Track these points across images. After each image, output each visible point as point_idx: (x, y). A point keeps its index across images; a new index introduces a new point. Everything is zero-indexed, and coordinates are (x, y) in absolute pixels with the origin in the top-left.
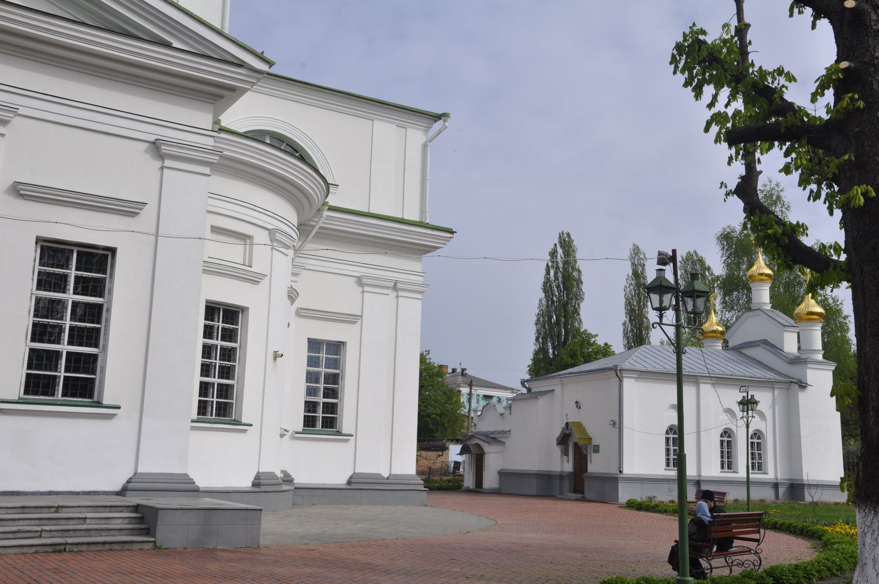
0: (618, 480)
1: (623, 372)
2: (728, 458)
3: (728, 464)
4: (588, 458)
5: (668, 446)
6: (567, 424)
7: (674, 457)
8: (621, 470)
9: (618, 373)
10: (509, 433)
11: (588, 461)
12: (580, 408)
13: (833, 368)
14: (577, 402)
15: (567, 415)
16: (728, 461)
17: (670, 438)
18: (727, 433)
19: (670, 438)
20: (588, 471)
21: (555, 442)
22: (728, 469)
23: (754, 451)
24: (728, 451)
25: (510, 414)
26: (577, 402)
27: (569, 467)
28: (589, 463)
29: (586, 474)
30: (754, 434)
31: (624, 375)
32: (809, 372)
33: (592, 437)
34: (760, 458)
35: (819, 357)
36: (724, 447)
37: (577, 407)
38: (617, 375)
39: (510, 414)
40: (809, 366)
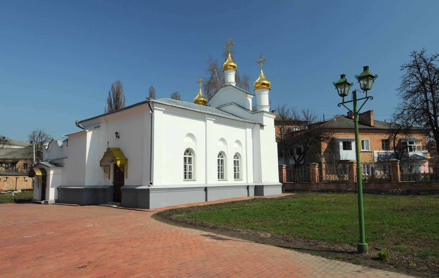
0: (149, 191)
1: (155, 104)
2: (221, 171)
4: (125, 175)
5: (185, 163)
6: (108, 149)
7: (189, 171)
8: (152, 182)
9: (151, 104)
10: (66, 159)
11: (125, 177)
12: (119, 137)
13: (274, 117)
14: (117, 133)
15: (108, 143)
16: (222, 173)
18: (221, 154)
20: (124, 185)
22: (189, 178)
23: (235, 166)
24: (221, 167)
25: (67, 146)
26: (117, 133)
27: (110, 182)
28: (125, 178)
29: (122, 187)
30: (235, 155)
31: (155, 107)
32: (264, 117)
33: (128, 159)
34: (238, 171)
35: (267, 110)
36: (219, 164)
37: (117, 137)
38: (149, 106)
39: (67, 146)
40: (265, 114)
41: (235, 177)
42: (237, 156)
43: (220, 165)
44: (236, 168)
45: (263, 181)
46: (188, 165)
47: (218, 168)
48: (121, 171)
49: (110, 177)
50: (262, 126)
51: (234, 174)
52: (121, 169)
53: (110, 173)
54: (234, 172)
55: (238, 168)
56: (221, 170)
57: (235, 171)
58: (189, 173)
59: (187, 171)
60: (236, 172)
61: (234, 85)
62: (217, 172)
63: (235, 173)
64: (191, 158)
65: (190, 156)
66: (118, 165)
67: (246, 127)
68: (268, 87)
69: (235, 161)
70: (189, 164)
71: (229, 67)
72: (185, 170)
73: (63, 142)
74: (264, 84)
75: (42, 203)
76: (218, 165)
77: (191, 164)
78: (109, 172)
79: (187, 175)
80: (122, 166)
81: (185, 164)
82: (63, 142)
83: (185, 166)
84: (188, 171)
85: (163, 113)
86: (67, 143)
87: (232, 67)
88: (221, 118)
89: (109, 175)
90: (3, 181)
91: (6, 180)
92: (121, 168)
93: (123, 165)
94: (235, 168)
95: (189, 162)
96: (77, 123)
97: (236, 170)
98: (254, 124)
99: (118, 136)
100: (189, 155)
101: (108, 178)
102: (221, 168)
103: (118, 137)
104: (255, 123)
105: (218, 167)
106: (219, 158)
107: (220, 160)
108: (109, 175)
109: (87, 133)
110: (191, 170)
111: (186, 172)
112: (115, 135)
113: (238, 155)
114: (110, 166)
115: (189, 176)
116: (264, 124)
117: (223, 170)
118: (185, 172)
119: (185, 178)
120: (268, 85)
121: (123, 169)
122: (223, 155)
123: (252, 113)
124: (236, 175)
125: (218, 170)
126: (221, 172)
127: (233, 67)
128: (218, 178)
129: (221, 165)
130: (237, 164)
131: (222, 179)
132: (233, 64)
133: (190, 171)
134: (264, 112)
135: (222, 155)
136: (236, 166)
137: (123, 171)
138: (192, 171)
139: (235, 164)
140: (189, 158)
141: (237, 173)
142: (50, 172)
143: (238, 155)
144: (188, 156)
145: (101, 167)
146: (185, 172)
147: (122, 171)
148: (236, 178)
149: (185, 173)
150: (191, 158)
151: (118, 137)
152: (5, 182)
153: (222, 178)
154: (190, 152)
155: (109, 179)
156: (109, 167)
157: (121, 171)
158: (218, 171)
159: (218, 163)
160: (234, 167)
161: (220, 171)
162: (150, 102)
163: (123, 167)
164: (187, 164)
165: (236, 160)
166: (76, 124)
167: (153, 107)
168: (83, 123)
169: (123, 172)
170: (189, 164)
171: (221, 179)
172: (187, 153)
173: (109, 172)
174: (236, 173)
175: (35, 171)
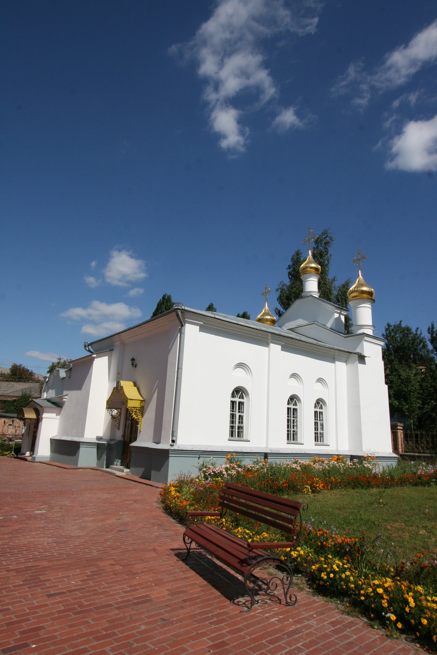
0: (169, 454)
2: (293, 428)
3: (293, 434)
5: (233, 411)
8: (174, 439)
9: (180, 313)
12: (136, 366)
17: (236, 402)
18: (293, 399)
19: (236, 402)
21: (104, 405)
23: (316, 421)
24: (294, 421)
26: (133, 360)
32: (365, 343)
34: (322, 429)
37: (133, 365)
38: (178, 315)
39: (70, 377)
40: (366, 338)
41: (316, 439)
42: (319, 403)
43: (291, 417)
44: (317, 423)
45: (364, 449)
46: (237, 414)
47: (288, 422)
48: (133, 417)
49: (119, 427)
50: (362, 358)
51: (315, 433)
52: (133, 414)
53: (120, 421)
54: (315, 430)
55: (322, 425)
56: (293, 426)
57: (316, 429)
58: (239, 428)
59: (235, 424)
60: (318, 430)
61: (317, 295)
62: (286, 429)
63: (316, 432)
64: (244, 402)
65: (241, 400)
66: (129, 409)
67: (336, 357)
68: (370, 297)
69: (316, 412)
70: (239, 412)
71: (309, 269)
72: (232, 422)
73: (65, 372)
74: (363, 292)
75: (28, 460)
76: (288, 417)
77: (243, 412)
78: (118, 419)
79: (235, 431)
80: (135, 410)
81: (233, 413)
82: (65, 372)
83: (233, 416)
84: (237, 424)
85: (200, 330)
86: (70, 373)
87: (312, 270)
88: (294, 341)
89: (118, 423)
90: (8, 424)
91: (11, 423)
92: (133, 413)
93: (137, 408)
94: (316, 424)
95: (239, 409)
96: (87, 345)
97: (317, 428)
98: (348, 354)
99: (135, 364)
100: (240, 398)
101: (117, 428)
102: (293, 423)
103: (134, 366)
104: (351, 353)
105: (288, 420)
106: (289, 406)
107: (291, 408)
108: (119, 424)
109: (96, 360)
110: (242, 423)
111: (234, 425)
112: (130, 363)
113: (321, 403)
114: (121, 409)
115: (238, 432)
116: (365, 355)
117: (297, 426)
118: (232, 425)
119: (232, 434)
120: (370, 293)
121: (136, 415)
122: (297, 401)
123: (345, 337)
124: (318, 436)
125: (288, 426)
126: (292, 430)
127: (316, 270)
128: (288, 439)
129: (293, 417)
130: (320, 418)
131: (294, 441)
132: (313, 265)
133: (241, 425)
134: (365, 335)
135: (295, 401)
136: (317, 420)
137: (136, 417)
138: (245, 425)
139: (317, 418)
140: (240, 403)
141: (320, 433)
142: (42, 415)
143: (321, 403)
144: (237, 400)
145: (108, 410)
146: (232, 425)
147: (134, 418)
148: (318, 441)
149: (232, 427)
150: (244, 402)
151: (134, 366)
152: (9, 426)
153: (293, 440)
154: (242, 394)
155: (119, 430)
156: (120, 410)
157: (133, 417)
158: (288, 427)
159: (288, 414)
160: (315, 422)
161: (291, 428)
162: (179, 310)
163: (136, 412)
164: (236, 412)
165: (319, 410)
166: (85, 346)
167: (184, 318)
168: (94, 345)
169: (136, 419)
170: (239, 412)
171: (292, 441)
172: (237, 394)
173: (118, 419)
174: (318, 433)
175: (25, 412)
